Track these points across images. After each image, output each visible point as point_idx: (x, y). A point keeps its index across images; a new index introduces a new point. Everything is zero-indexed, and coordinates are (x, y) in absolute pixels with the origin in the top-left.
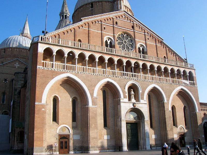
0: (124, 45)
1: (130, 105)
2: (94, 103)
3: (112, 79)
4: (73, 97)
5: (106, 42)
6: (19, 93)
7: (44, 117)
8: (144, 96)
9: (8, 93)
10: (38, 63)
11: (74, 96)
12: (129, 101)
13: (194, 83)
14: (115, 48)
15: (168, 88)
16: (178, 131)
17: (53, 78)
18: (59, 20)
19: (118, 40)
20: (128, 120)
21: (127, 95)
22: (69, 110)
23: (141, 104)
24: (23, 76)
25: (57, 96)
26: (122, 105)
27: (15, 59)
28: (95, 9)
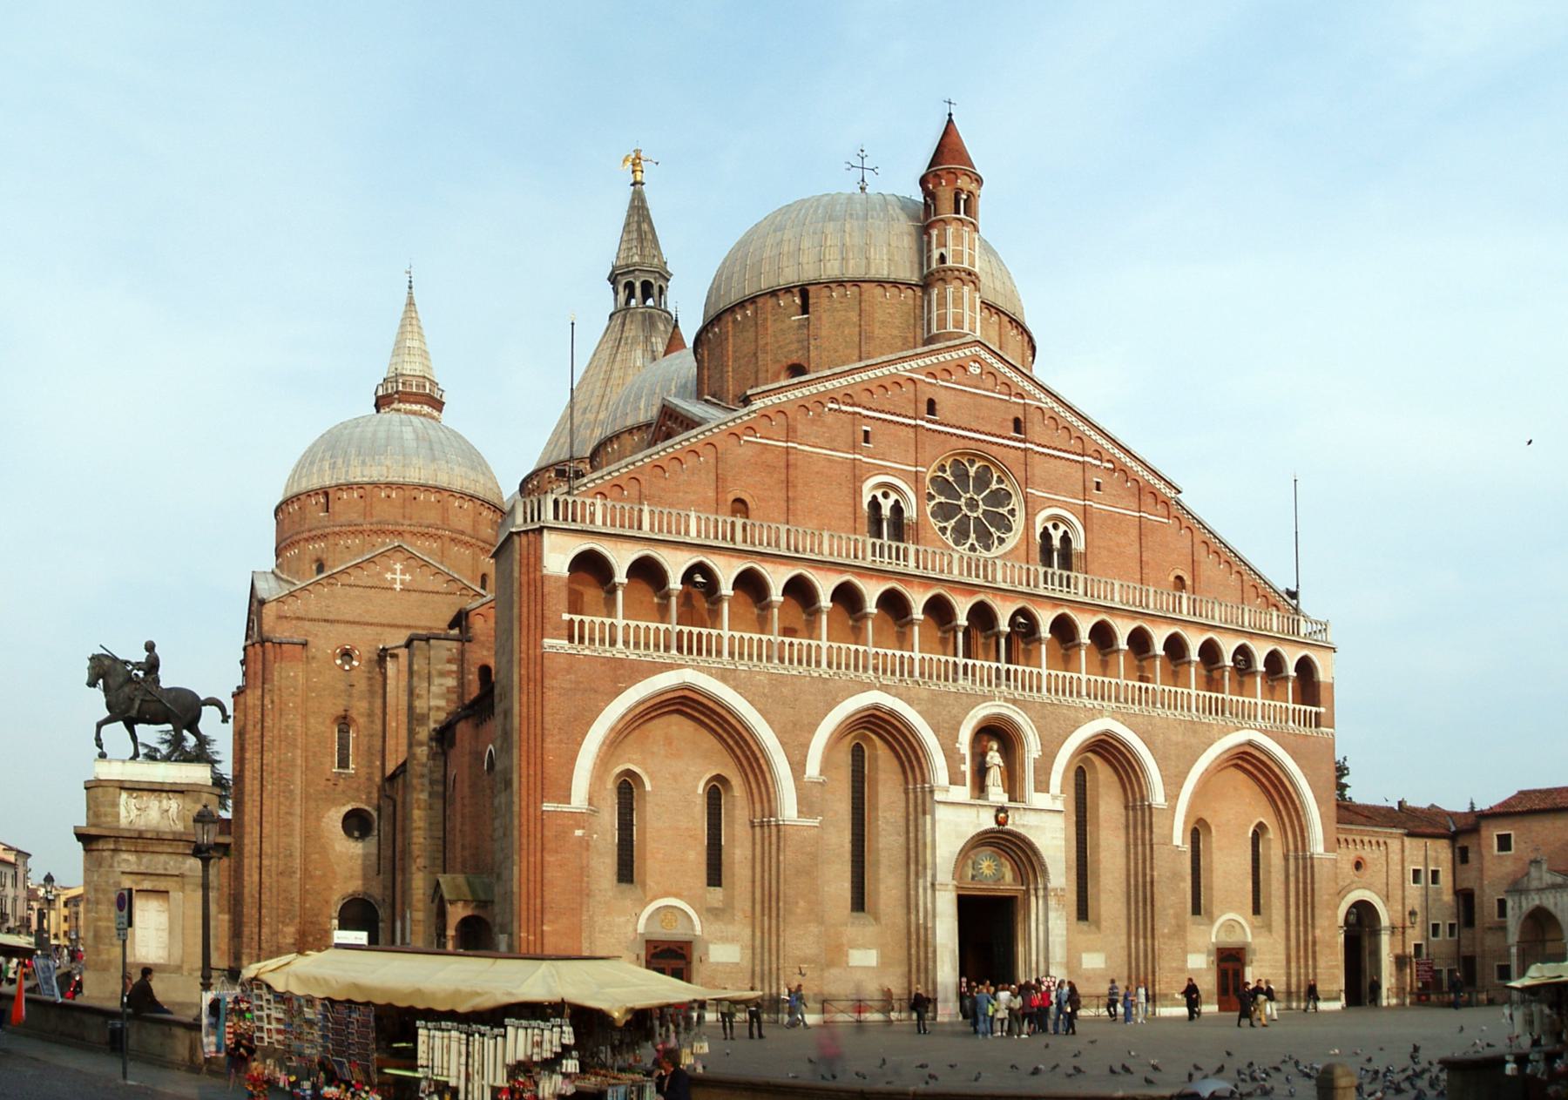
2: (806, 805)
3: (895, 696)
4: (708, 776)
5: (875, 505)
6: (444, 736)
7: (585, 862)
8: (1053, 773)
11: (714, 773)
14: (916, 542)
15: (1180, 738)
19: (933, 492)
21: (967, 768)
22: (690, 836)
24: (450, 650)
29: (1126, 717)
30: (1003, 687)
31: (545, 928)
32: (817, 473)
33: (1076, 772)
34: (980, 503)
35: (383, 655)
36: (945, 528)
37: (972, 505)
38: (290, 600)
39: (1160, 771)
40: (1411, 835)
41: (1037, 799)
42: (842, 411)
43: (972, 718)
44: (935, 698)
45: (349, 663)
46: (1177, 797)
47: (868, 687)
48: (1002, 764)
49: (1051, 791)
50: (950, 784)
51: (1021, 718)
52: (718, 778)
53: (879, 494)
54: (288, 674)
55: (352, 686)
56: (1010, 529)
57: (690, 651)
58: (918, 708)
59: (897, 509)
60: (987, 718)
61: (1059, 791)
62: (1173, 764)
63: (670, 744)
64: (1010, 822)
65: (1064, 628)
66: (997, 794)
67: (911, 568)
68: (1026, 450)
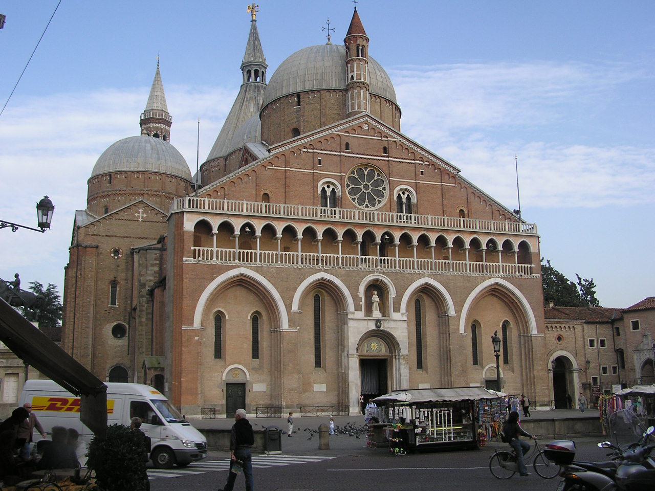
1: (368, 325)
3: (331, 274)
5: (324, 191)
6: (151, 293)
9: (122, 282)
10: (185, 253)
12: (365, 316)
15: (462, 284)
16: (484, 377)
18: (242, 83)
19: (349, 183)
20: (365, 353)
21: (363, 303)
23: (392, 322)
25: (223, 311)
26: (351, 324)
27: (135, 199)
28: (304, 108)
31: (182, 379)
32: (298, 180)
33: (416, 301)
35: (132, 252)
37: (366, 187)
38: (91, 226)
40: (587, 323)
41: (395, 316)
43: (364, 282)
44: (348, 274)
45: (117, 256)
47: (319, 271)
48: (379, 301)
51: (387, 280)
54: (90, 261)
55: (118, 266)
57: (243, 261)
58: (341, 279)
60: (371, 281)
61: (404, 311)
62: (459, 296)
64: (382, 326)
65: (406, 239)
67: (337, 219)
68: (389, 161)
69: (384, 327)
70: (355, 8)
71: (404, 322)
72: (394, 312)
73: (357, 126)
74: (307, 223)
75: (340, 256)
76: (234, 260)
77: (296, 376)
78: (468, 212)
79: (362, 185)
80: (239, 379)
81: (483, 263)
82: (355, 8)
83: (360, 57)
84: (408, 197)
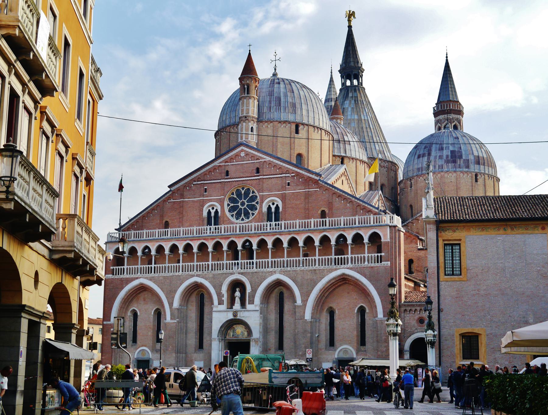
0: (241, 209)
1: (227, 315)
4: (155, 309)
5: (209, 213)
13: (381, 256)
15: (309, 277)
17: (123, 288)
19: (229, 203)
21: (225, 298)
26: (215, 315)
29: (285, 272)
30: (240, 269)
34: (246, 202)
36: (233, 215)
37: (243, 204)
39: (300, 291)
42: (198, 184)
44: (214, 276)
46: (307, 300)
47: (193, 276)
49: (255, 303)
50: (219, 304)
52: (157, 309)
53: (210, 209)
56: (256, 209)
59: (217, 212)
63: (145, 300)
64: (238, 316)
66: (237, 306)
69: (240, 316)
70: (250, 51)
71: (256, 312)
72: (249, 304)
73: (234, 156)
74: (186, 240)
75: (210, 263)
76: (137, 273)
77: (174, 355)
78: (329, 211)
79: (240, 203)
80: (145, 357)
81: (332, 257)
82: (250, 51)
83: (246, 95)
84: (277, 205)
